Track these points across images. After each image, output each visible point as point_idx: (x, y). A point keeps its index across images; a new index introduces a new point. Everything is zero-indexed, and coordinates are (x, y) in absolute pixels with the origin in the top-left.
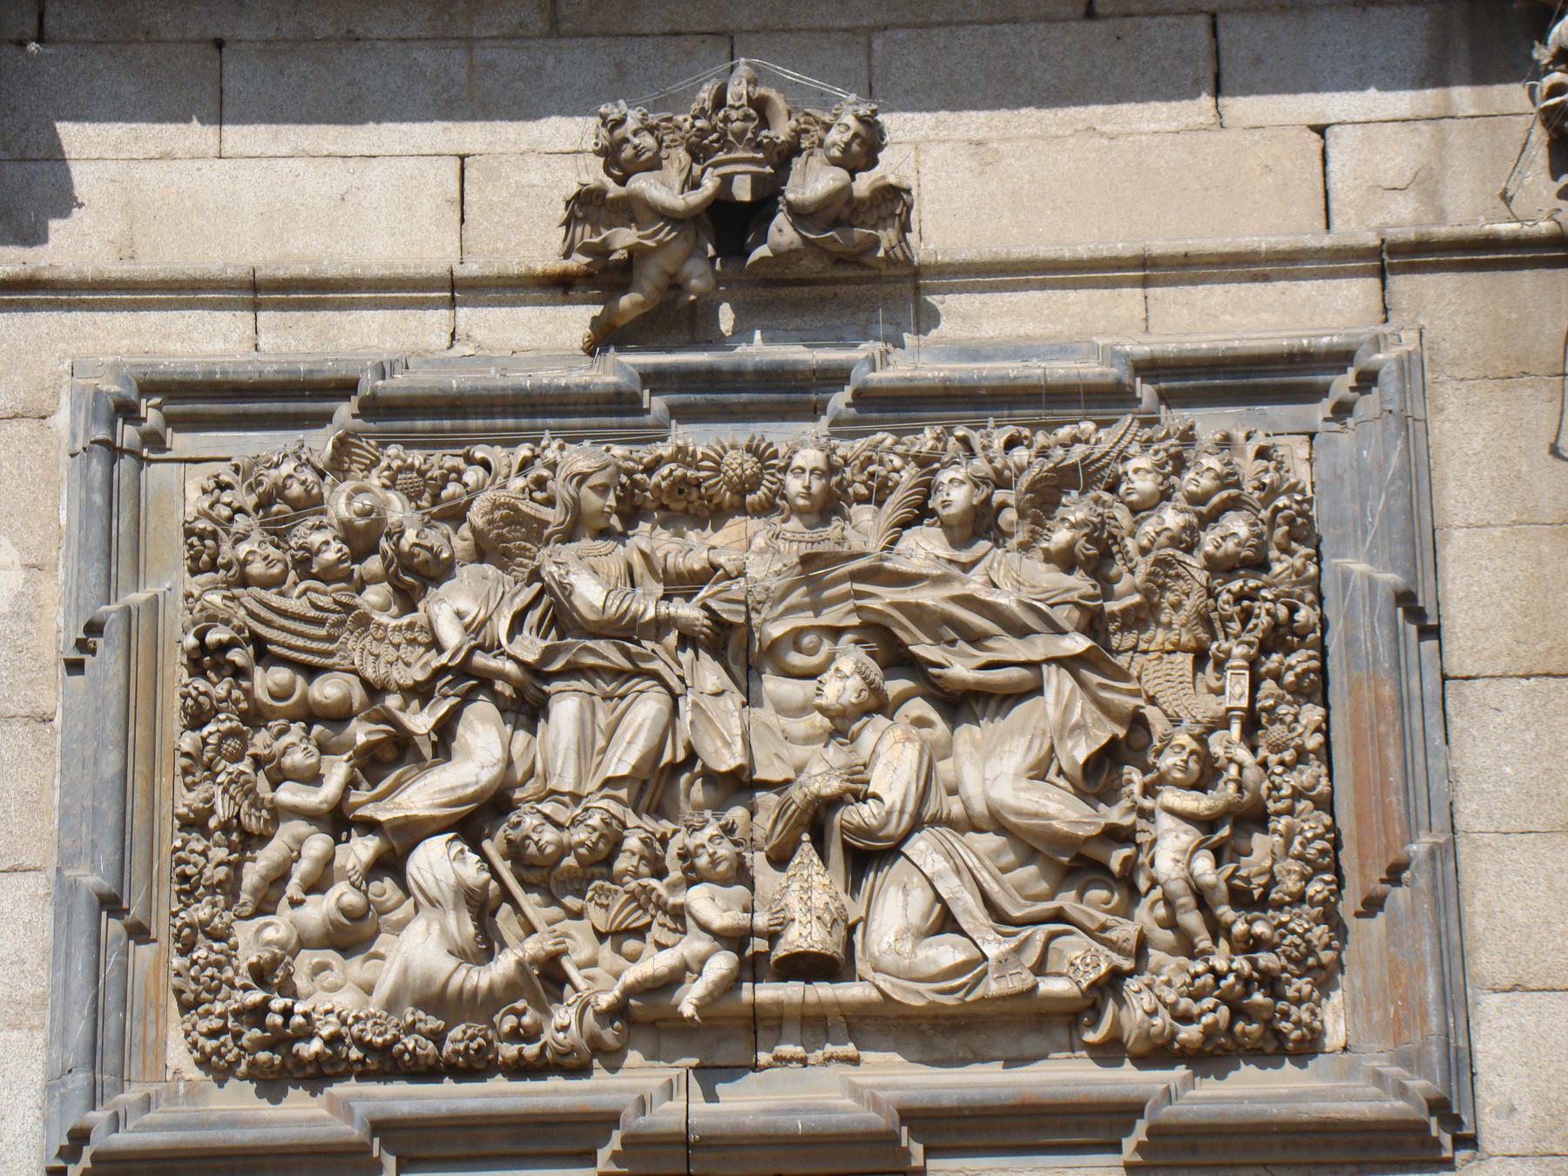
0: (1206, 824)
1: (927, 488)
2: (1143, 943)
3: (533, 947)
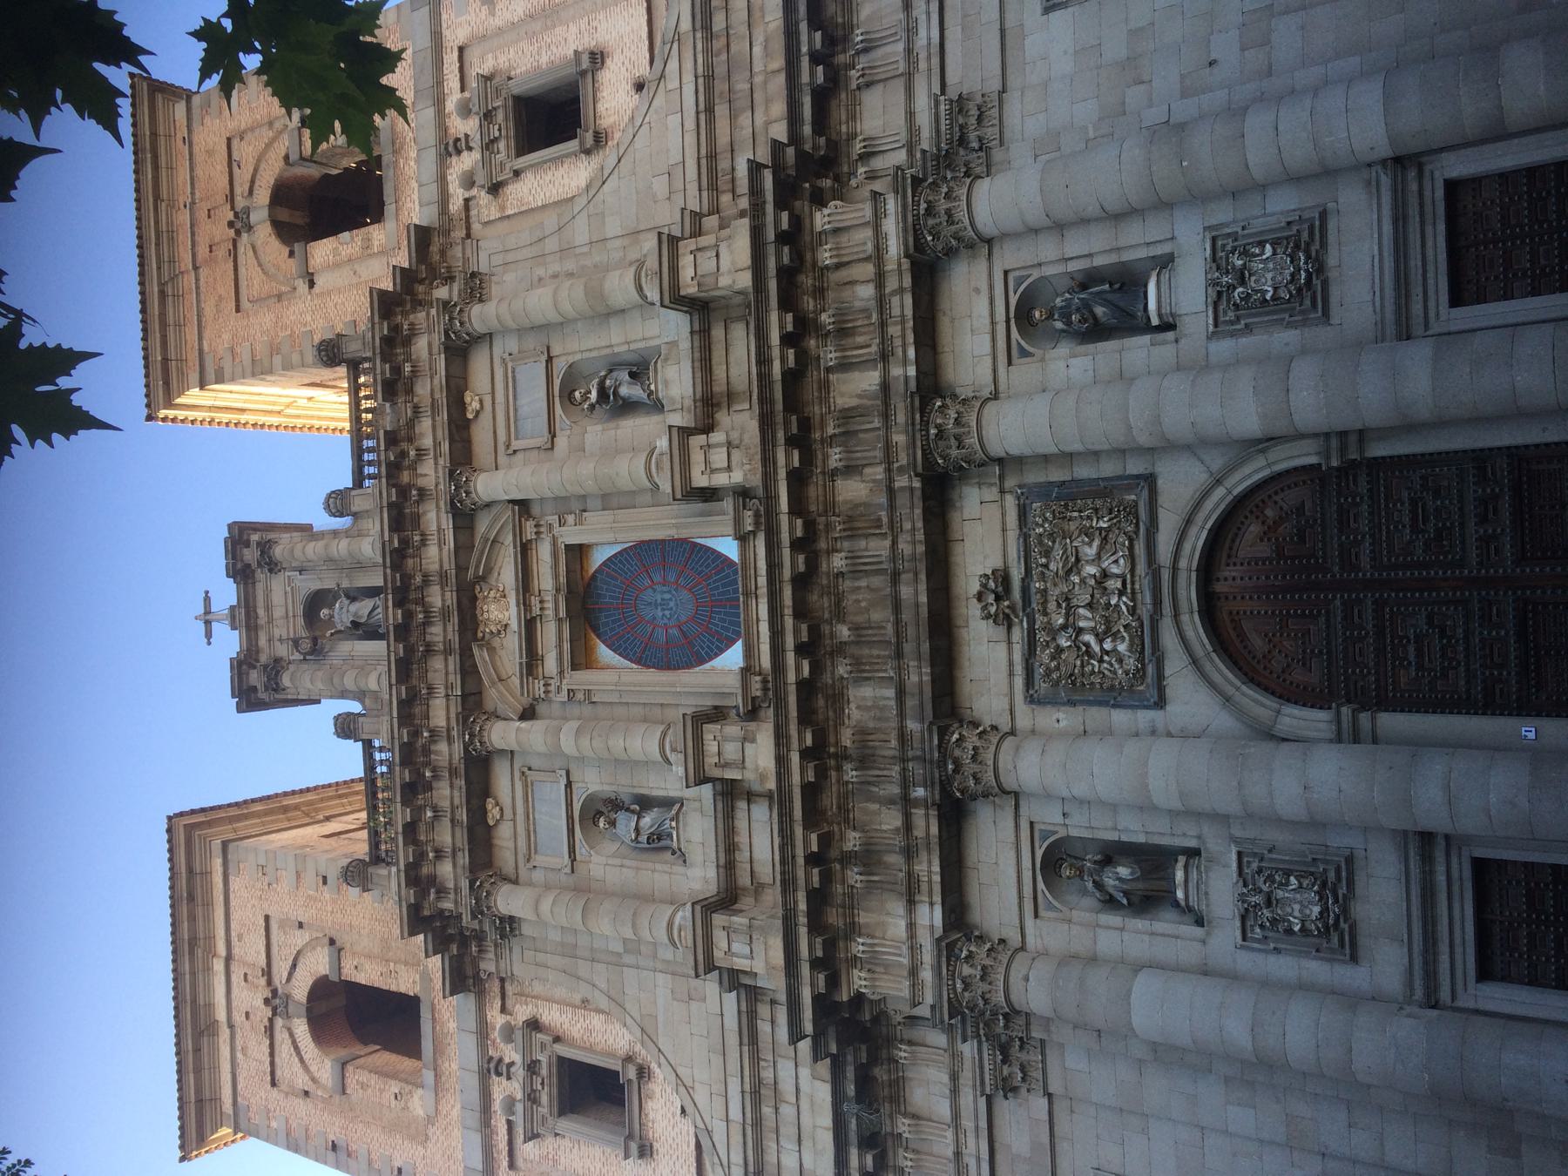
0: (1098, 518)
1: (1042, 565)
2: (1118, 528)
3: (1122, 630)
